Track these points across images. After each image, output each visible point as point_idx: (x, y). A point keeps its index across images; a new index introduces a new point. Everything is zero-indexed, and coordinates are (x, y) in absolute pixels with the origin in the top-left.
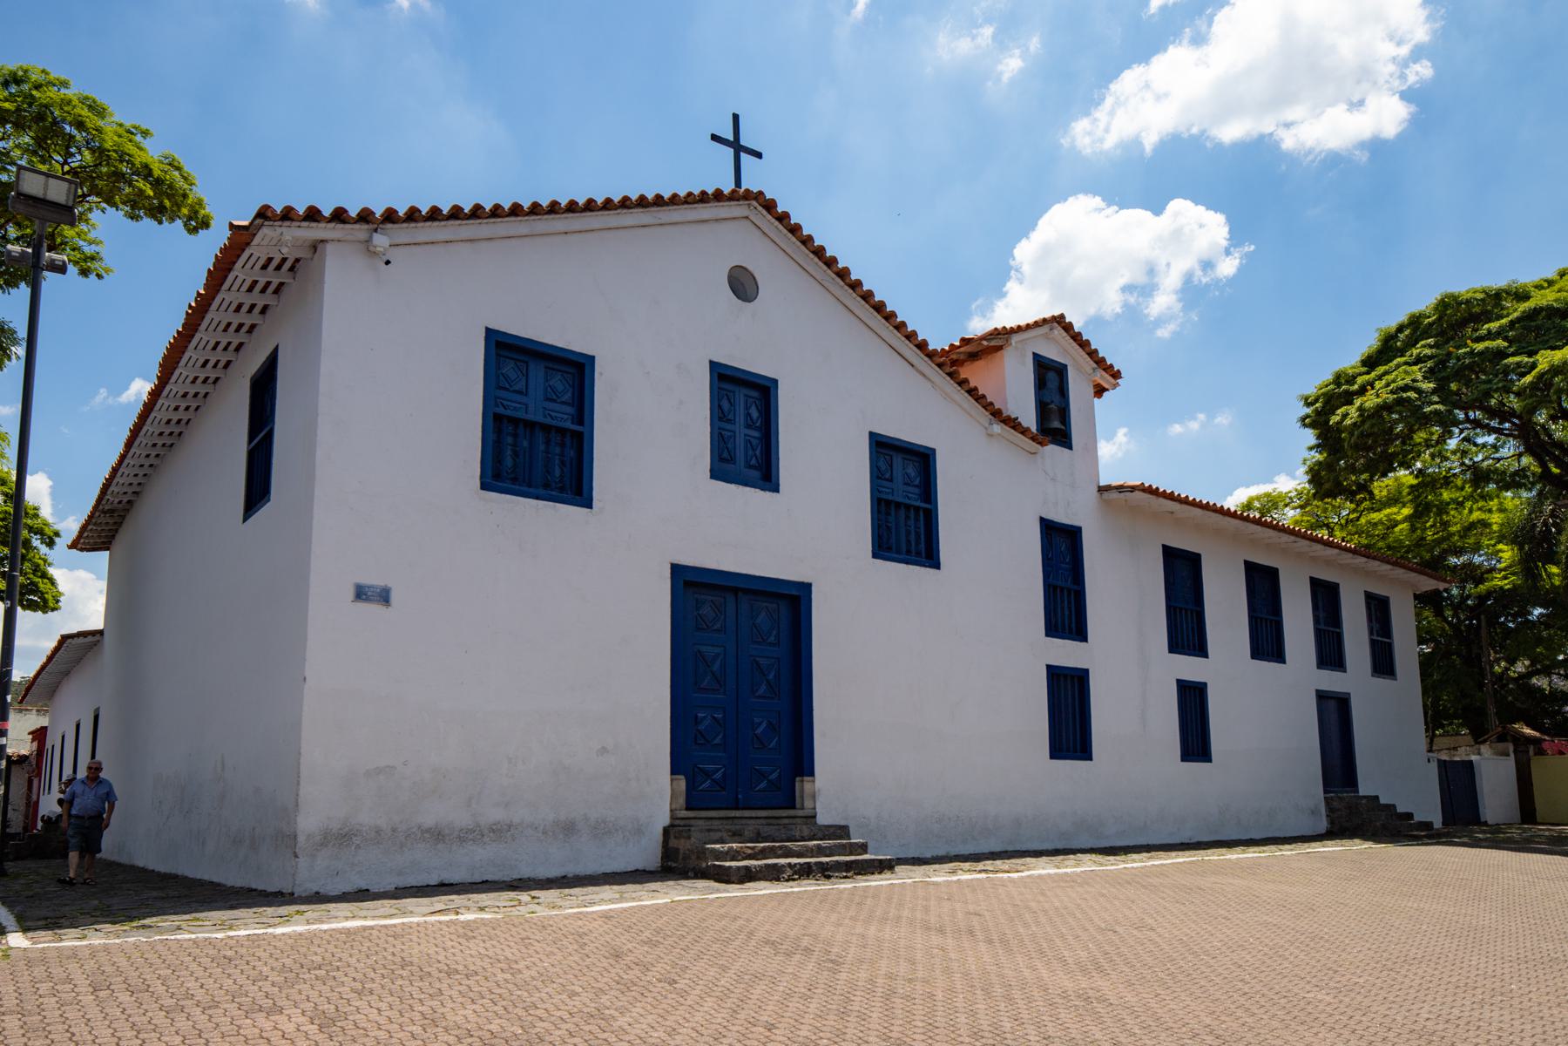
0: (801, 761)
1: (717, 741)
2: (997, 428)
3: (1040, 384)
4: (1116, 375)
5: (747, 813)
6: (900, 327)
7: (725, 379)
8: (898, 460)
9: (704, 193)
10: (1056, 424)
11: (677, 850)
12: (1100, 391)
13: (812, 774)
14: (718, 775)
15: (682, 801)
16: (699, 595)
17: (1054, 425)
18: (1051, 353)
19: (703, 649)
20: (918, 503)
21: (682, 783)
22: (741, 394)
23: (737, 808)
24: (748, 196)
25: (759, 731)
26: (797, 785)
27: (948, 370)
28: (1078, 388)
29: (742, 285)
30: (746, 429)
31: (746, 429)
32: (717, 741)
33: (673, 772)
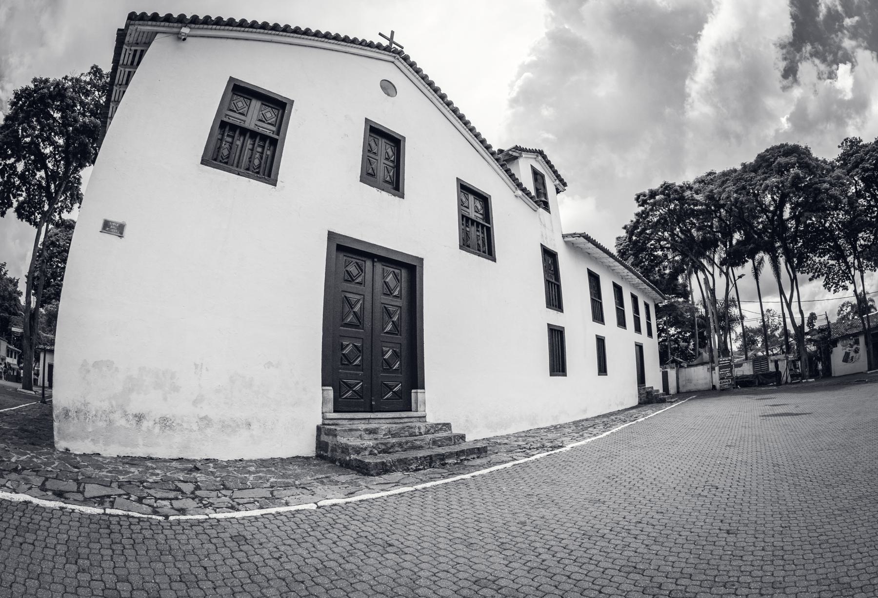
0: (414, 378)
1: (357, 362)
2: (520, 193)
3: (536, 180)
4: (565, 184)
5: (379, 415)
6: (472, 130)
7: (375, 131)
8: (471, 197)
9: (371, 42)
10: (543, 199)
11: (327, 444)
12: (558, 191)
13: (424, 388)
14: (358, 387)
15: (331, 406)
16: (345, 252)
17: (541, 201)
18: (539, 168)
19: (348, 295)
20: (481, 222)
21: (330, 392)
22: (382, 142)
23: (371, 412)
24: (395, 52)
25: (386, 357)
26: (413, 395)
27: (496, 157)
28: (550, 185)
29: (388, 88)
30: (384, 159)
31: (384, 159)
32: (357, 362)
33: (323, 385)
